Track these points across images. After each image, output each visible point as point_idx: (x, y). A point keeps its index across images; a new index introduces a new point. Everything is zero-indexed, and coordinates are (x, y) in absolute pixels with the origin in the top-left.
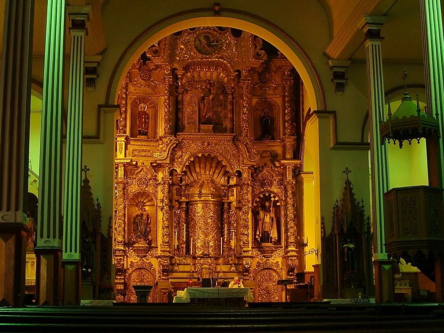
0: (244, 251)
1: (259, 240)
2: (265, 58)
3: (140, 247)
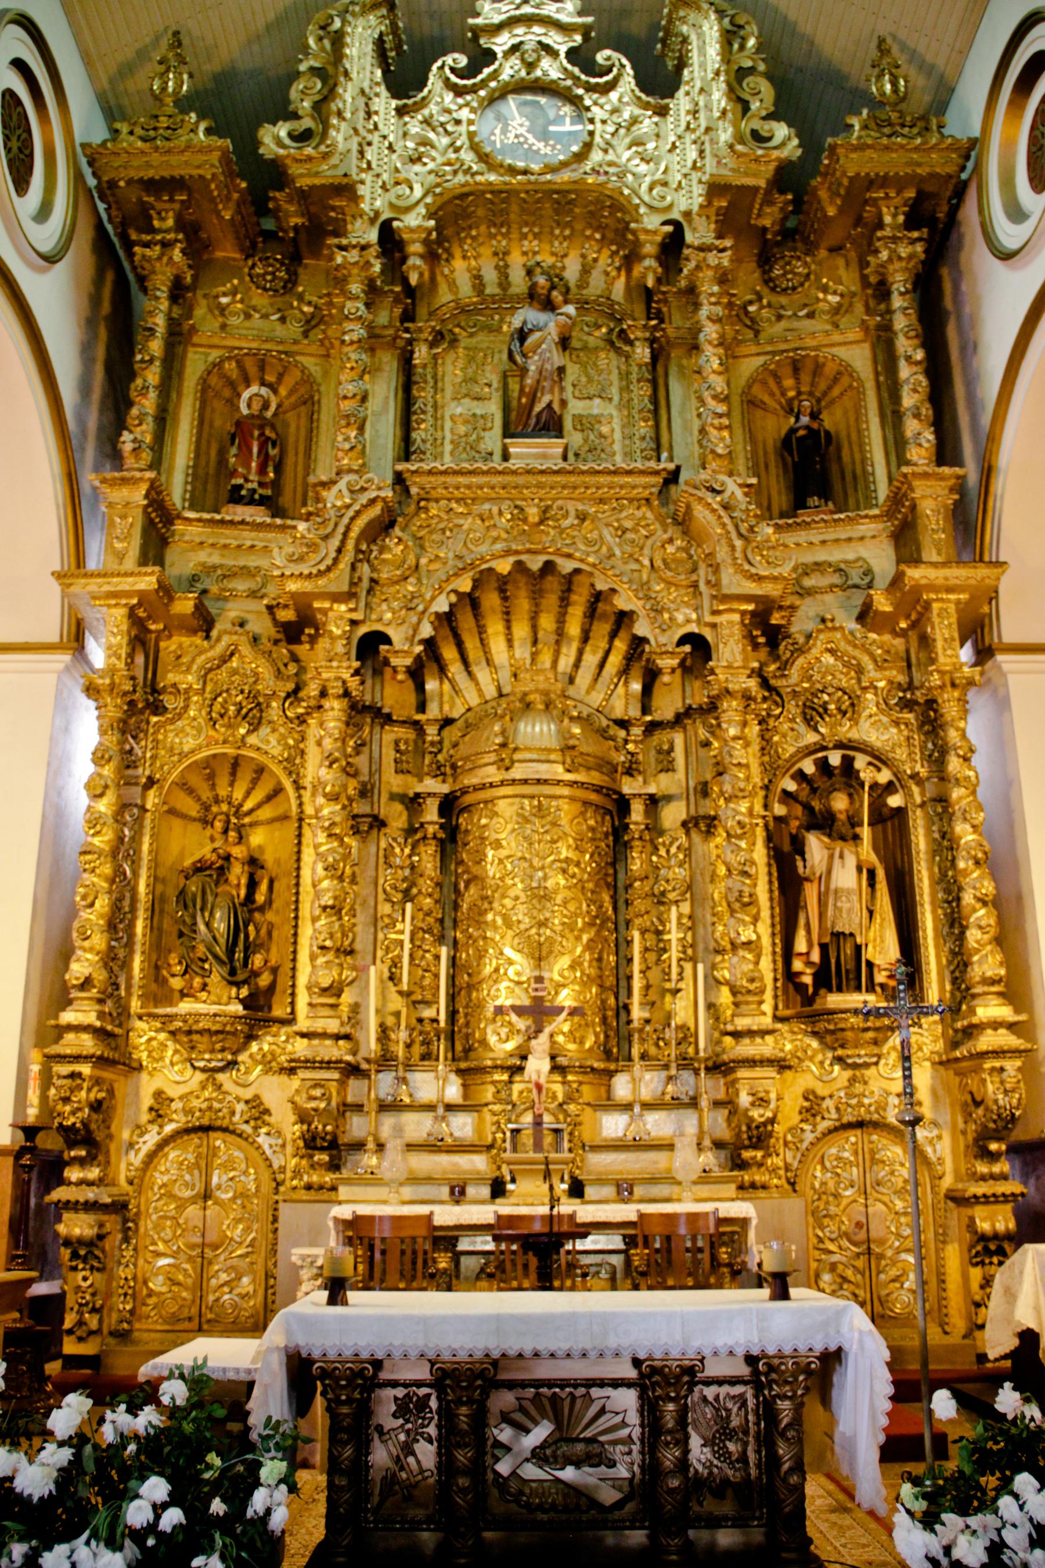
0: (736, 1035)
1: (808, 979)
2: (792, 150)
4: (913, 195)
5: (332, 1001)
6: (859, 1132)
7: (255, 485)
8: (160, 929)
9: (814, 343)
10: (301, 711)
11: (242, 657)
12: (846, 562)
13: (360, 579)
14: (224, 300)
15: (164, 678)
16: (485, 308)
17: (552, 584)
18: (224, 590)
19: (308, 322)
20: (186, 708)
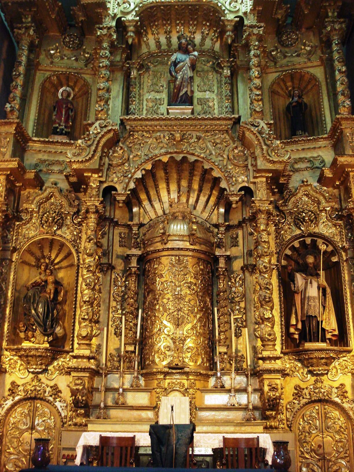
0: (264, 359)
1: (296, 336)
3: (30, 349)
4: (341, 4)
5: (87, 342)
6: (319, 405)
7: (63, 127)
8: (17, 312)
9: (300, 67)
10: (79, 220)
11: (56, 197)
12: (313, 157)
13: (104, 164)
14: (52, 52)
15: (22, 206)
16: (162, 54)
17: (186, 166)
18: (49, 170)
19: (87, 61)
20: (31, 219)
